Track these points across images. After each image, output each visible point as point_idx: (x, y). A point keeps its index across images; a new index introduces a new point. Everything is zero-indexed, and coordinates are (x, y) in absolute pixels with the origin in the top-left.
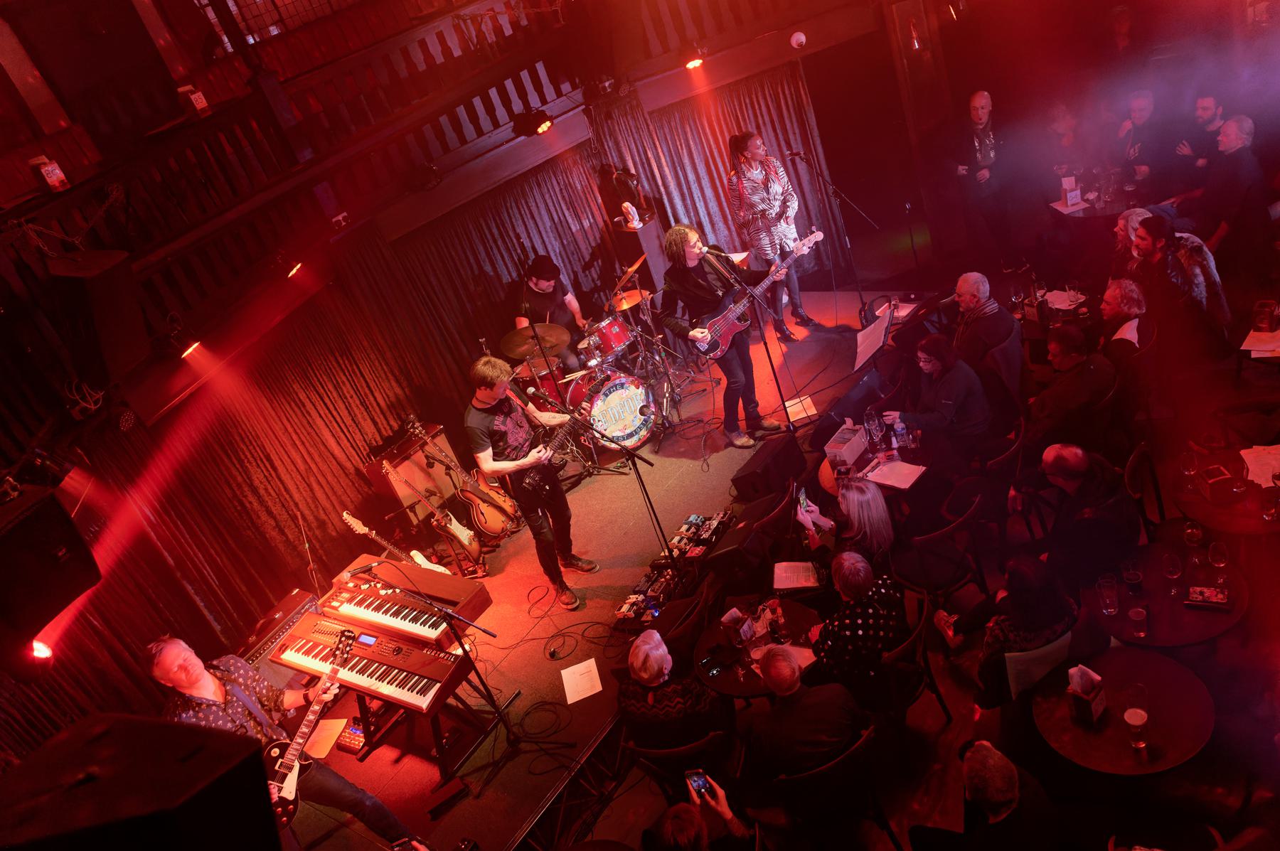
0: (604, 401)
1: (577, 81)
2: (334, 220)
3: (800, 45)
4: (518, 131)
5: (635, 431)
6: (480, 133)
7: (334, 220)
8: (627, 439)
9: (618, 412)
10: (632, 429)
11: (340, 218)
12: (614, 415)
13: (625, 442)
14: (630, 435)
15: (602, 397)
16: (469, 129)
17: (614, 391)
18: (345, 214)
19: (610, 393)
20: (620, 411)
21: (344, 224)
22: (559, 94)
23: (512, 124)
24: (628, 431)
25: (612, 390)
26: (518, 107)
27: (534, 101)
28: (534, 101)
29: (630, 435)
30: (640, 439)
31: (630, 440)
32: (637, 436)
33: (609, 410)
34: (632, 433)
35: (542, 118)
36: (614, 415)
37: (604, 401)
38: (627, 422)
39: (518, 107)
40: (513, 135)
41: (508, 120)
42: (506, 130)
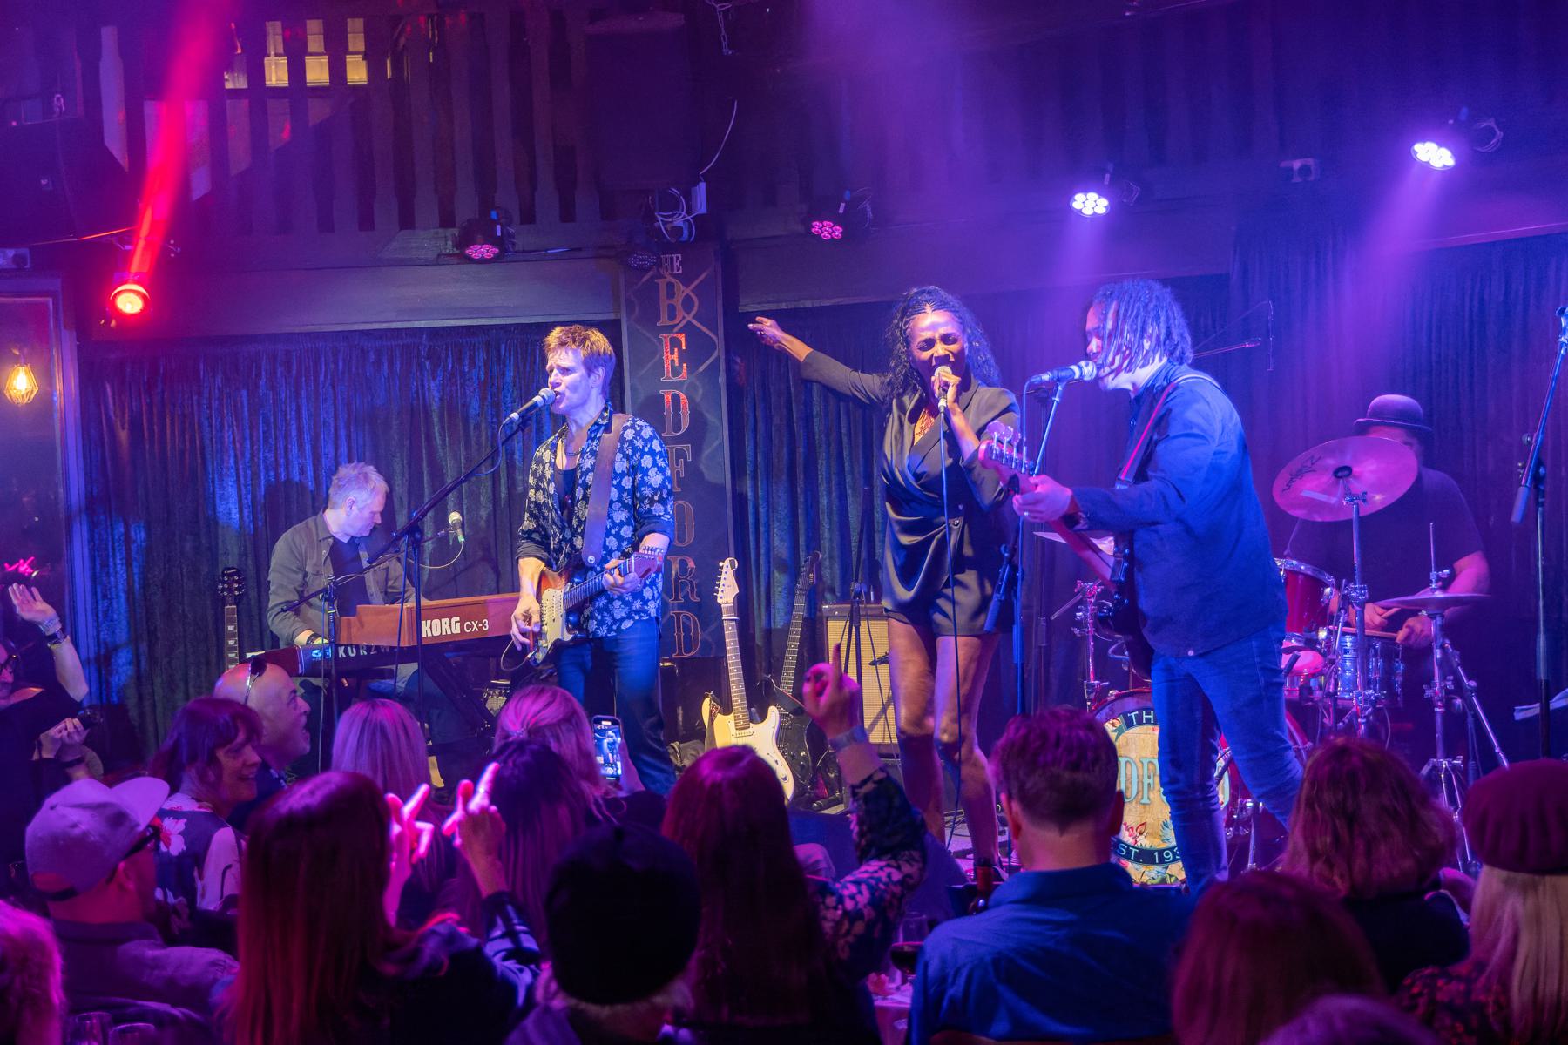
0: (1120, 731)
2: (1283, 165)
5: (1161, 852)
7: (1283, 165)
8: (1137, 860)
9: (1140, 782)
11: (1297, 165)
15: (1119, 721)
17: (1148, 721)
18: (1310, 161)
19: (1140, 722)
20: (1146, 781)
21: (1297, 179)
24: (1144, 842)
25: (1144, 716)
30: (1164, 880)
31: (1142, 868)
32: (1159, 868)
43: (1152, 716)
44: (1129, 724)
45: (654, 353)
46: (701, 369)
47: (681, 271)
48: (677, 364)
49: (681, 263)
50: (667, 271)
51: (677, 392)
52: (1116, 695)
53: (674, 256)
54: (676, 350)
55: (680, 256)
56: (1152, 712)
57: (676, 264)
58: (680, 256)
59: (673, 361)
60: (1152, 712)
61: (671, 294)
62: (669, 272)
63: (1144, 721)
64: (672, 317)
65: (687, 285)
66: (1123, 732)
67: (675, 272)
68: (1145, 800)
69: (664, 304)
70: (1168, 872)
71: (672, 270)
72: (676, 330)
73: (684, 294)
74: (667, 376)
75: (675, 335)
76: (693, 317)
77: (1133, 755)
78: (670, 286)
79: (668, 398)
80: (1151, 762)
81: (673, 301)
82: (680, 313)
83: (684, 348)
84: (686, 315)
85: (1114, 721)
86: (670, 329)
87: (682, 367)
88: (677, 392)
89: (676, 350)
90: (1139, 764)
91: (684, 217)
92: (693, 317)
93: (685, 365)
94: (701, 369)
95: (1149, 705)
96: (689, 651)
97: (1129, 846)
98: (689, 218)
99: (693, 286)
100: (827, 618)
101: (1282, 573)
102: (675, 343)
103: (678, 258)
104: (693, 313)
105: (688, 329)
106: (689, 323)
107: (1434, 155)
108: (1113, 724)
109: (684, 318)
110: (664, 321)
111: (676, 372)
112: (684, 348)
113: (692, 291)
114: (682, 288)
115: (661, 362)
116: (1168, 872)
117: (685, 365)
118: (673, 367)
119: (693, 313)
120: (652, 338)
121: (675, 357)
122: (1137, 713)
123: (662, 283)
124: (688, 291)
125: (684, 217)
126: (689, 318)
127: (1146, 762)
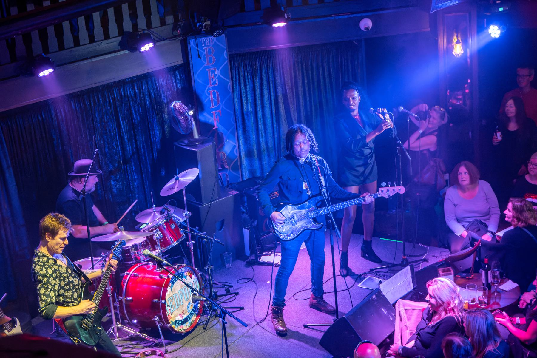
0: (172, 287)
1: (180, 15)
3: (367, 29)
4: (123, 46)
5: (189, 316)
6: (92, 40)
8: (184, 323)
9: (180, 299)
10: (187, 314)
12: (177, 301)
13: (183, 326)
14: (186, 320)
16: (83, 34)
19: (176, 281)
22: (163, 23)
23: (120, 38)
24: (185, 316)
26: (128, 26)
27: (142, 24)
28: (142, 24)
29: (186, 320)
30: (191, 324)
33: (174, 296)
34: (187, 318)
35: (146, 38)
36: (177, 301)
38: (184, 308)
39: (128, 26)
40: (119, 48)
41: (117, 35)
42: (114, 42)
44: (173, 283)
68: (182, 304)
70: (192, 320)
77: (176, 292)
80: (181, 291)
90: (178, 294)
97: (181, 320)
107: (46, 72)
108: (170, 286)
116: (192, 320)
127: (179, 292)
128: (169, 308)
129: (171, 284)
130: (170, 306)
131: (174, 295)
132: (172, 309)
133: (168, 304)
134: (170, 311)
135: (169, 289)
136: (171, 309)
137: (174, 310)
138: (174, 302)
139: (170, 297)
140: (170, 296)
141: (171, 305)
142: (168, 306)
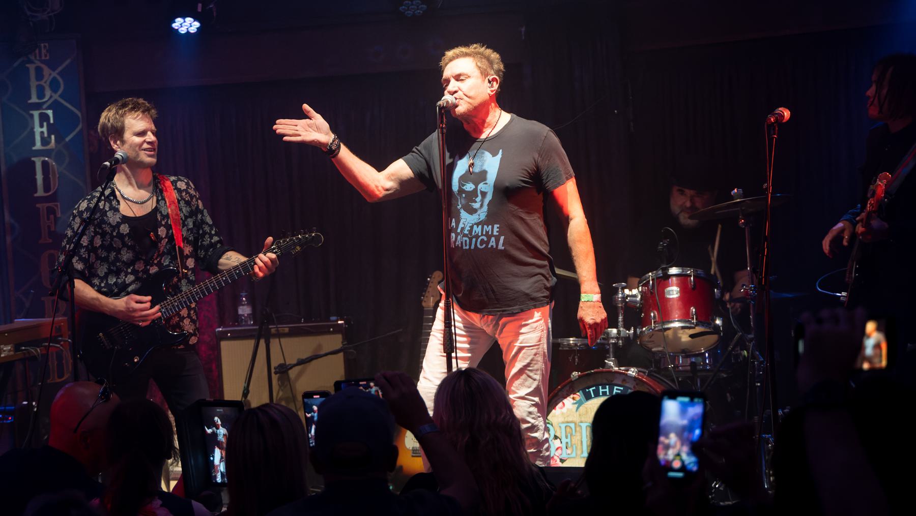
0: (580, 404)
25: (601, 390)
37: (580, 404)
43: (607, 390)
45: (27, 125)
46: (67, 139)
47: (48, 58)
48: (46, 135)
49: (47, 51)
50: (35, 57)
51: (47, 159)
52: (579, 376)
53: (42, 45)
54: (45, 124)
55: (47, 44)
56: (607, 387)
57: (44, 51)
58: (47, 44)
59: (42, 133)
60: (607, 387)
61: (39, 75)
62: (38, 58)
63: (601, 394)
64: (41, 95)
65: (54, 70)
66: (583, 403)
67: (43, 58)
69: (33, 84)
71: (40, 56)
72: (45, 106)
73: (52, 77)
74: (38, 145)
75: (44, 111)
76: (61, 96)
78: (39, 71)
79: (38, 161)
81: (42, 83)
82: (48, 93)
83: (52, 121)
84: (53, 94)
85: (575, 396)
86: (37, 106)
87: (49, 136)
88: (47, 159)
89: (45, 124)
91: (49, 13)
92: (61, 96)
93: (53, 137)
94: (67, 139)
95: (605, 381)
96: (60, 377)
98: (51, 14)
99: (60, 69)
100: (220, 341)
101: (692, 278)
102: (44, 118)
103: (45, 47)
104: (60, 92)
105: (55, 106)
106: (56, 101)
108: (573, 398)
109: (51, 97)
110: (34, 99)
111: (45, 141)
112: (52, 121)
113: (58, 74)
114: (52, 72)
115: (32, 133)
117: (53, 137)
118: (42, 138)
119: (60, 92)
120: (24, 114)
121: (45, 129)
122: (594, 388)
123: (32, 68)
124: (54, 74)
125: (49, 13)
126: (56, 96)
128: (557, 443)
129: (579, 396)
130: (564, 440)
131: (581, 422)
132: (569, 451)
133: (558, 435)
134: (559, 451)
135: (568, 402)
136: (564, 448)
137: (574, 455)
138: (579, 438)
139: (568, 422)
140: (570, 419)
141: (568, 440)
142: (556, 437)
